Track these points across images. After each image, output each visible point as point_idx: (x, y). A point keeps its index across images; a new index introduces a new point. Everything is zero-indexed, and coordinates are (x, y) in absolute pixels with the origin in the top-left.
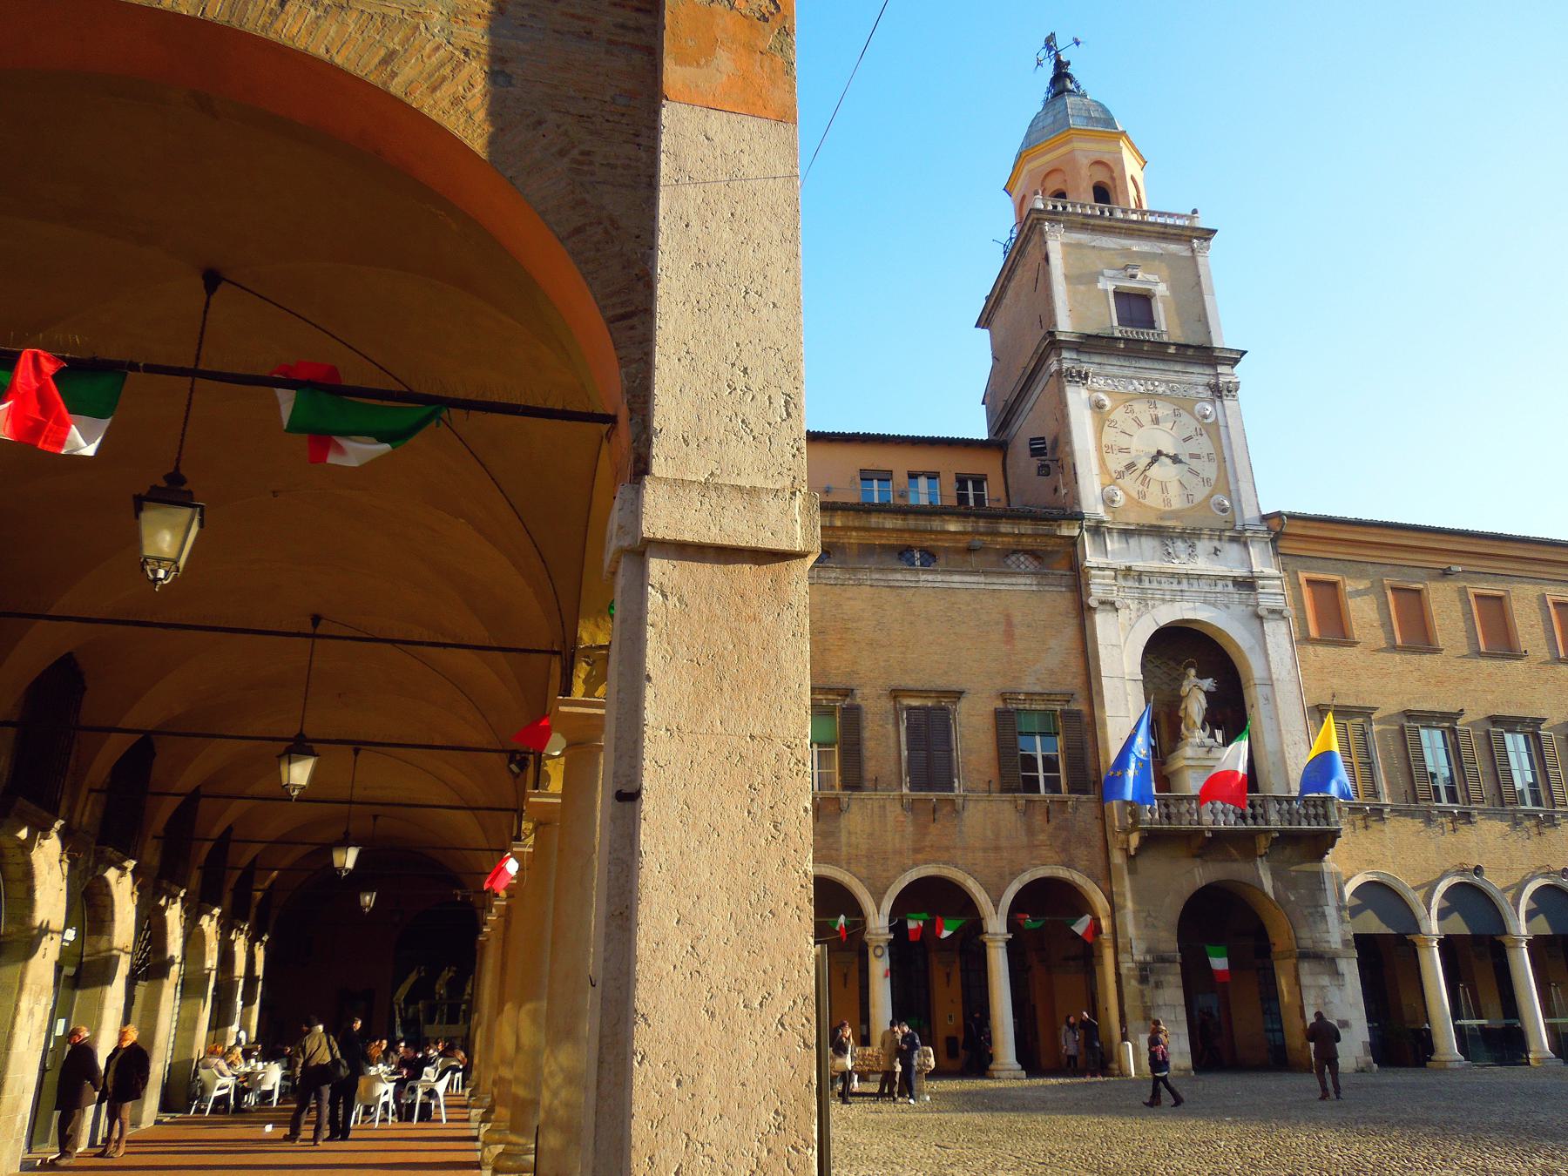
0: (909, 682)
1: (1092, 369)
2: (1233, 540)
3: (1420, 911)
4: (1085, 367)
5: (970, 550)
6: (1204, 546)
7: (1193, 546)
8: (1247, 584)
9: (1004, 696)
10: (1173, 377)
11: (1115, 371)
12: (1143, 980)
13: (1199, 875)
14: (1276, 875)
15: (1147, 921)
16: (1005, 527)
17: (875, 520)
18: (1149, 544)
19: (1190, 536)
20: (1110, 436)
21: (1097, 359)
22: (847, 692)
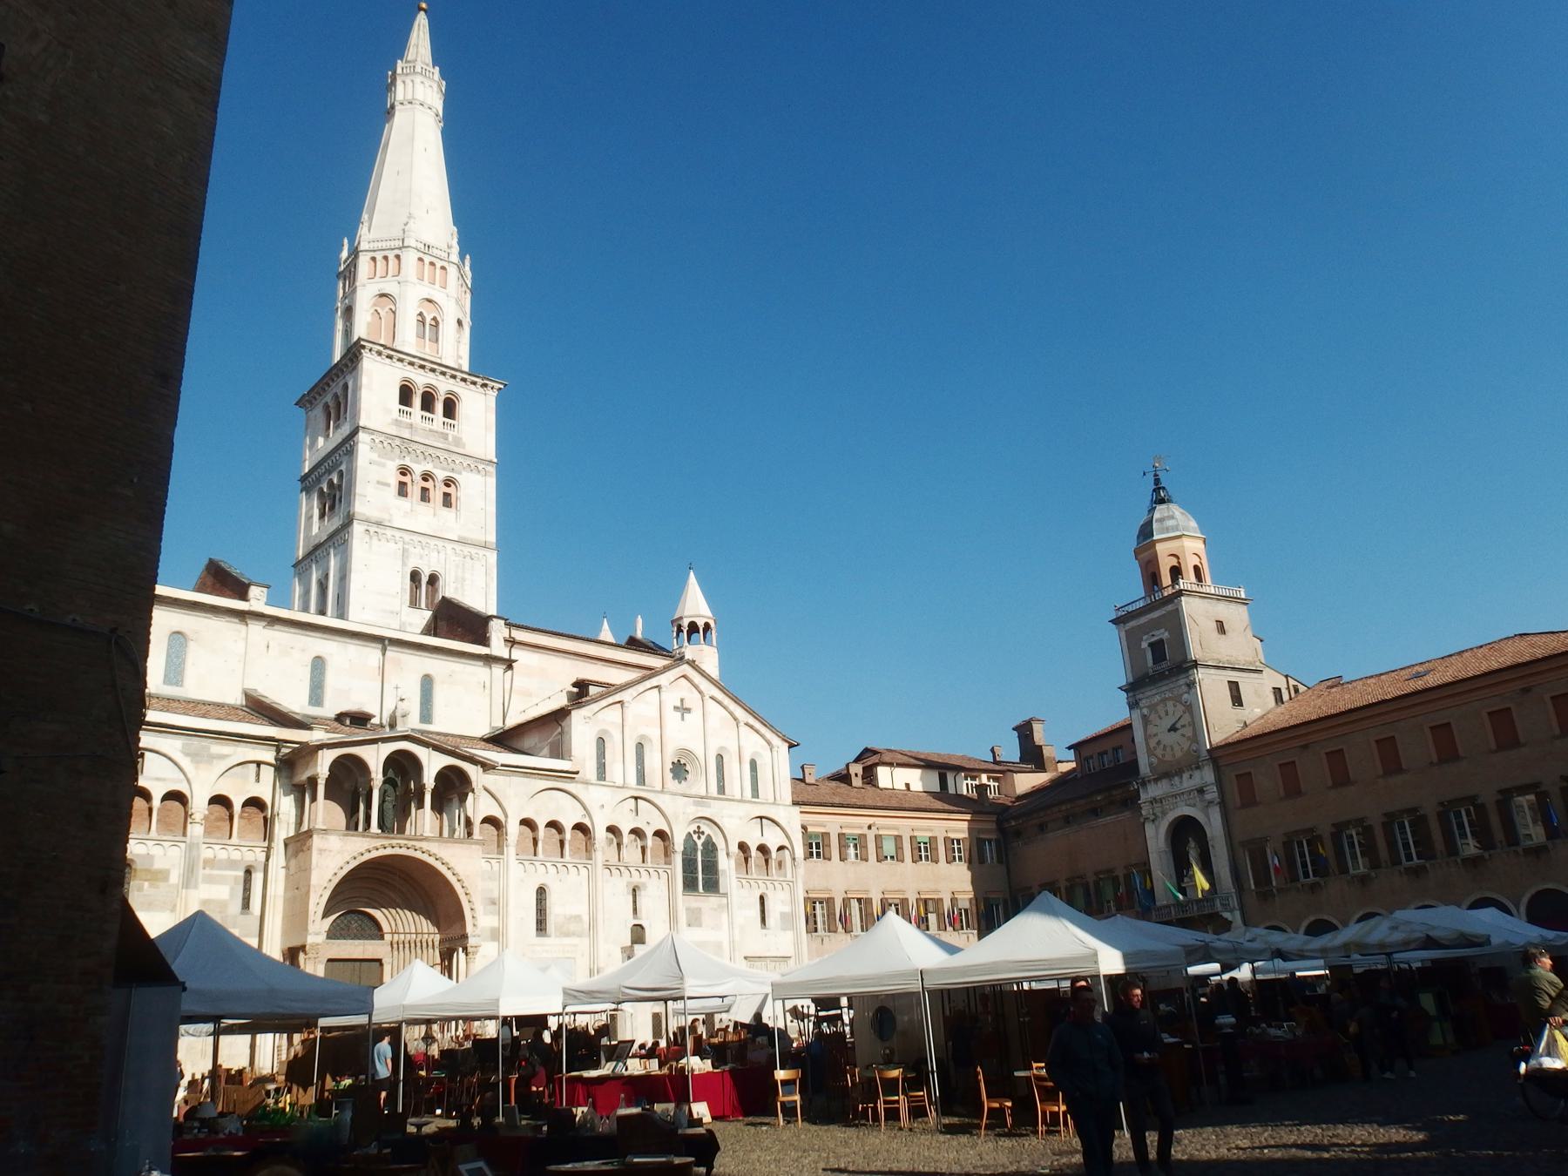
2: (1198, 768)
6: (1186, 776)
8: (1201, 791)
19: (1179, 773)
20: (1152, 730)
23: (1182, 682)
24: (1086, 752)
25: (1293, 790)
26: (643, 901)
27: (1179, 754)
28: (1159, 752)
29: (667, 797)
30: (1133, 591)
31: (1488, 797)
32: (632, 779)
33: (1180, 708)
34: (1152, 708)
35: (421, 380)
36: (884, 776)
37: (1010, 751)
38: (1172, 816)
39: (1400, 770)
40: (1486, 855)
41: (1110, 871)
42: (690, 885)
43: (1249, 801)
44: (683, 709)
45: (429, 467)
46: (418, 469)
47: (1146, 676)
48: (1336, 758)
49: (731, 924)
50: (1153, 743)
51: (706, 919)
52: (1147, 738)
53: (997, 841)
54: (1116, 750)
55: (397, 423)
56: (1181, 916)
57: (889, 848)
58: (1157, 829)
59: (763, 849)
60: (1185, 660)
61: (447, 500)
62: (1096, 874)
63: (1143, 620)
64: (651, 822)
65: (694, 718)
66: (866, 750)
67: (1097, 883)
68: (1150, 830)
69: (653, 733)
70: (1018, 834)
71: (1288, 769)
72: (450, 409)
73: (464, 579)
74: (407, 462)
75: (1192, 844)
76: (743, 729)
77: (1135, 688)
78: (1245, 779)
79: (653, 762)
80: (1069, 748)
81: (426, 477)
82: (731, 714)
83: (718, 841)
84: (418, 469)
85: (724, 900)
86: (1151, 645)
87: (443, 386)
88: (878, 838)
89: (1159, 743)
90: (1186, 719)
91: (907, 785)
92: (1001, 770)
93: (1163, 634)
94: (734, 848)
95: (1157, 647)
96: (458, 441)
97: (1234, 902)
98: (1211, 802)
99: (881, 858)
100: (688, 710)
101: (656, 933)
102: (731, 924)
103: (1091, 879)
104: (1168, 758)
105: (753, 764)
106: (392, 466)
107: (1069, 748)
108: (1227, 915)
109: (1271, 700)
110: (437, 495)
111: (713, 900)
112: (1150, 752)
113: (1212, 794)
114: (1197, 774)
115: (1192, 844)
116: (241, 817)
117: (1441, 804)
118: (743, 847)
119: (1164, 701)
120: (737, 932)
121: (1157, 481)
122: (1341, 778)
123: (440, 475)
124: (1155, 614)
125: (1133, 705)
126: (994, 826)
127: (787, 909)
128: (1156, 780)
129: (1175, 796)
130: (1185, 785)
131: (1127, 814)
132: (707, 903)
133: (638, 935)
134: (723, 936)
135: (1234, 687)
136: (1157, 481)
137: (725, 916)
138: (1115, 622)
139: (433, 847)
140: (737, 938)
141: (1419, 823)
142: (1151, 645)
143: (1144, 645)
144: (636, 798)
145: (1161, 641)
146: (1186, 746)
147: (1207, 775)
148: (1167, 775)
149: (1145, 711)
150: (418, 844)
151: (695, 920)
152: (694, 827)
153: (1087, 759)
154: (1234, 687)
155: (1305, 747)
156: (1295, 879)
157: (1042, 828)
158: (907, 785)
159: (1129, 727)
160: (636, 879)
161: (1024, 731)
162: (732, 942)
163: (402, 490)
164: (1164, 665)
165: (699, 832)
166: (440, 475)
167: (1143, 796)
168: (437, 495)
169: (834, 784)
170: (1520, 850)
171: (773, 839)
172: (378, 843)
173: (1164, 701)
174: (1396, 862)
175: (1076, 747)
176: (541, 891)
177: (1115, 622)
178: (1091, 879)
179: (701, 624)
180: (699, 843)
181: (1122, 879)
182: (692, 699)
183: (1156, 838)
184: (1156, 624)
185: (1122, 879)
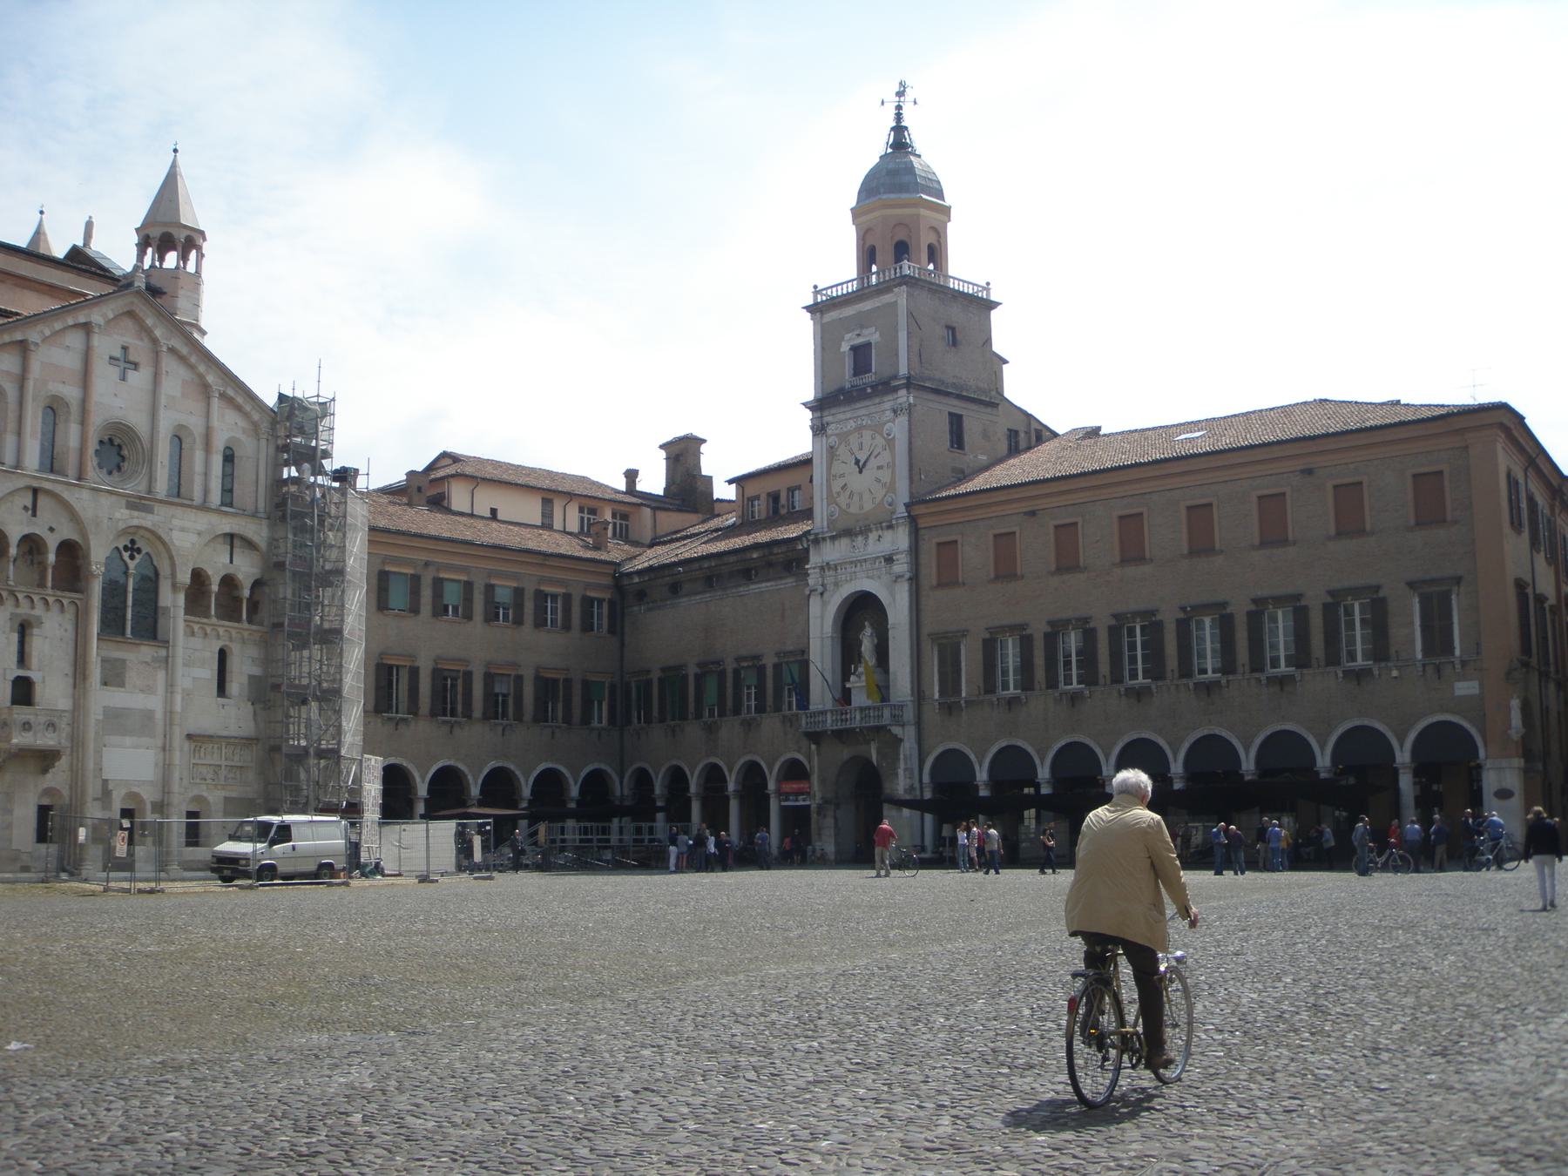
0: (744, 652)
1: (829, 419)
2: (890, 527)
3: (977, 767)
4: (826, 419)
5: (770, 565)
6: (873, 536)
7: (867, 538)
8: (889, 560)
9: (777, 654)
10: (873, 409)
11: (842, 416)
12: (819, 813)
13: (845, 753)
14: (878, 753)
15: (822, 781)
16: (776, 550)
17: (726, 559)
18: (845, 541)
19: (865, 531)
20: (838, 468)
21: (833, 411)
22: (718, 663)
23: (887, 405)
24: (752, 489)
25: (1006, 570)
26: (39, 645)
27: (868, 506)
28: (843, 500)
29: (85, 494)
30: (838, 264)
31: (1240, 608)
32: (32, 459)
33: (880, 441)
34: (843, 437)
36: (459, 498)
37: (654, 481)
38: (847, 590)
39: (1141, 559)
40: (1224, 681)
41: (757, 657)
42: (112, 624)
43: (949, 578)
44: (126, 362)
47: (841, 390)
48: (1066, 534)
49: (170, 686)
50: (836, 487)
51: (132, 676)
52: (830, 477)
53: (611, 603)
54: (791, 490)
56: (839, 726)
57: (452, 596)
58: (824, 604)
59: (229, 582)
60: (895, 377)
62: (738, 659)
63: (849, 311)
64: (53, 530)
65: (139, 379)
66: (444, 455)
67: (736, 672)
68: (815, 605)
69: (71, 393)
70: (641, 595)
71: (1004, 541)
75: (868, 631)
76: (215, 402)
77: (822, 406)
78: (948, 548)
79: (71, 436)
80: (730, 482)
82: (201, 377)
83: (165, 570)
85: (163, 652)
86: (855, 349)
88: (438, 584)
89: (844, 487)
90: (885, 457)
91: (494, 511)
92: (631, 501)
93: (872, 335)
94: (185, 577)
95: (861, 354)
97: (909, 714)
98: (898, 577)
99: (440, 610)
100: (136, 366)
101: (53, 691)
102: (170, 686)
103: (730, 666)
104: (854, 509)
105: (229, 458)
107: (730, 482)
108: (896, 730)
109: (1003, 447)
111: (147, 651)
112: (831, 499)
113: (902, 566)
114: (888, 535)
115: (868, 631)
117: (1183, 609)
118: (198, 576)
119: (859, 429)
120: (178, 698)
121: (899, 117)
122: (1067, 563)
124: (867, 306)
125: (818, 429)
126: (607, 581)
128: (833, 538)
129: (854, 563)
130: (870, 549)
131: (790, 582)
132: (137, 656)
133: (23, 691)
134: (155, 703)
135: (956, 422)
136: (899, 117)
137: (161, 676)
138: (808, 308)
140: (178, 708)
141: (1154, 629)
142: (855, 349)
143: (845, 347)
145: (868, 345)
146: (880, 493)
147: (899, 540)
148: (848, 533)
149: (833, 440)
151: (114, 676)
152: (124, 541)
153: (752, 499)
154: (956, 422)
155: (1033, 513)
156: (989, 688)
157: (675, 589)
158: (494, 511)
159: (804, 463)
160: (24, 609)
161: (682, 453)
162: (169, 713)
164: (869, 378)
165: (133, 549)
167: (815, 559)
169: (385, 499)
170: (1263, 677)
173: (859, 429)
174: (1117, 678)
175: (739, 481)
177: (808, 308)
178: (730, 666)
179: (181, 236)
180: (132, 564)
181: (769, 672)
182: (140, 349)
183: (822, 620)
184: (861, 322)
185: (769, 672)
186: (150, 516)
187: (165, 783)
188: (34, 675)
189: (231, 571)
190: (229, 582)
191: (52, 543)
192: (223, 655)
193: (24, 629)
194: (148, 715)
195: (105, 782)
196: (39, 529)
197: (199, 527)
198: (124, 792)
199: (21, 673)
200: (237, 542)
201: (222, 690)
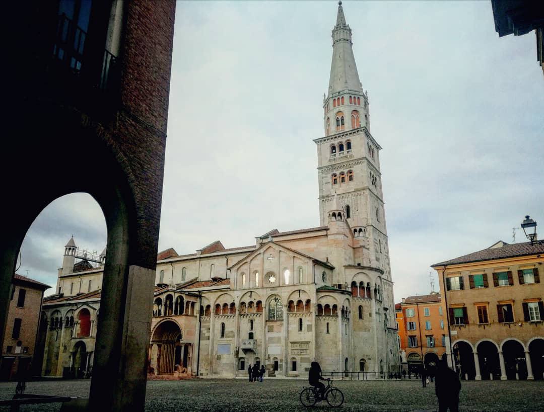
35: (336, 142)
45: (342, 170)
46: (338, 173)
51: (275, 329)
55: (330, 160)
59: (300, 302)
61: (351, 178)
64: (255, 299)
72: (349, 146)
73: (357, 204)
74: (335, 172)
81: (342, 174)
84: (338, 173)
87: (343, 140)
94: (285, 303)
96: (351, 156)
106: (329, 176)
110: (347, 178)
116: (359, 287)
118: (291, 302)
123: (346, 171)
127: (310, 323)
139: (174, 318)
144: (251, 292)
150: (171, 318)
151: (271, 330)
163: (335, 182)
166: (346, 171)
168: (347, 178)
171: (304, 298)
172: (163, 318)
176: (223, 325)
186: (276, 291)
187: (287, 354)
188: (253, 332)
189: (299, 299)
190: (300, 302)
191: (255, 302)
192: (301, 320)
193: (252, 322)
194: (279, 338)
195: (269, 355)
196: (253, 300)
197: (288, 290)
198: (273, 357)
199: (251, 332)
200: (301, 291)
201: (301, 329)
